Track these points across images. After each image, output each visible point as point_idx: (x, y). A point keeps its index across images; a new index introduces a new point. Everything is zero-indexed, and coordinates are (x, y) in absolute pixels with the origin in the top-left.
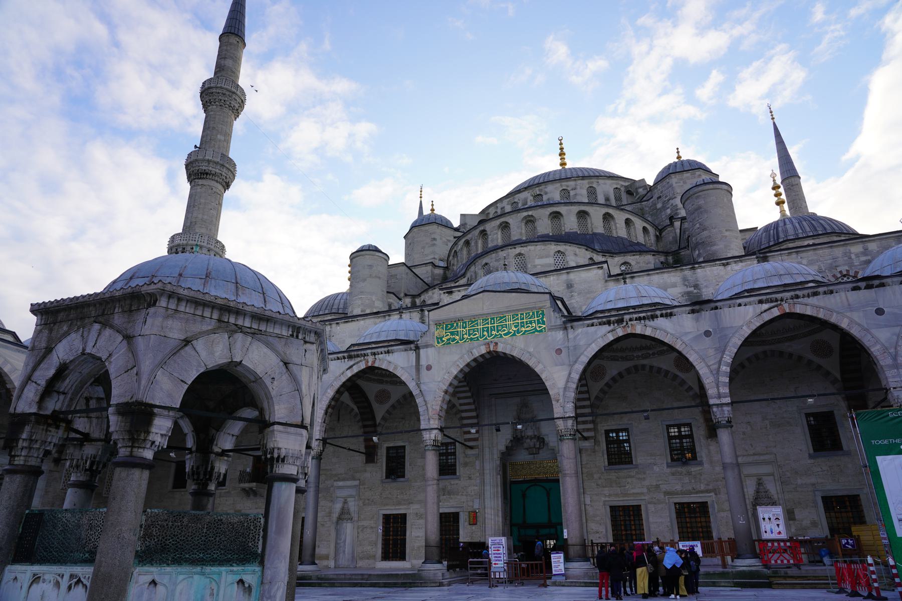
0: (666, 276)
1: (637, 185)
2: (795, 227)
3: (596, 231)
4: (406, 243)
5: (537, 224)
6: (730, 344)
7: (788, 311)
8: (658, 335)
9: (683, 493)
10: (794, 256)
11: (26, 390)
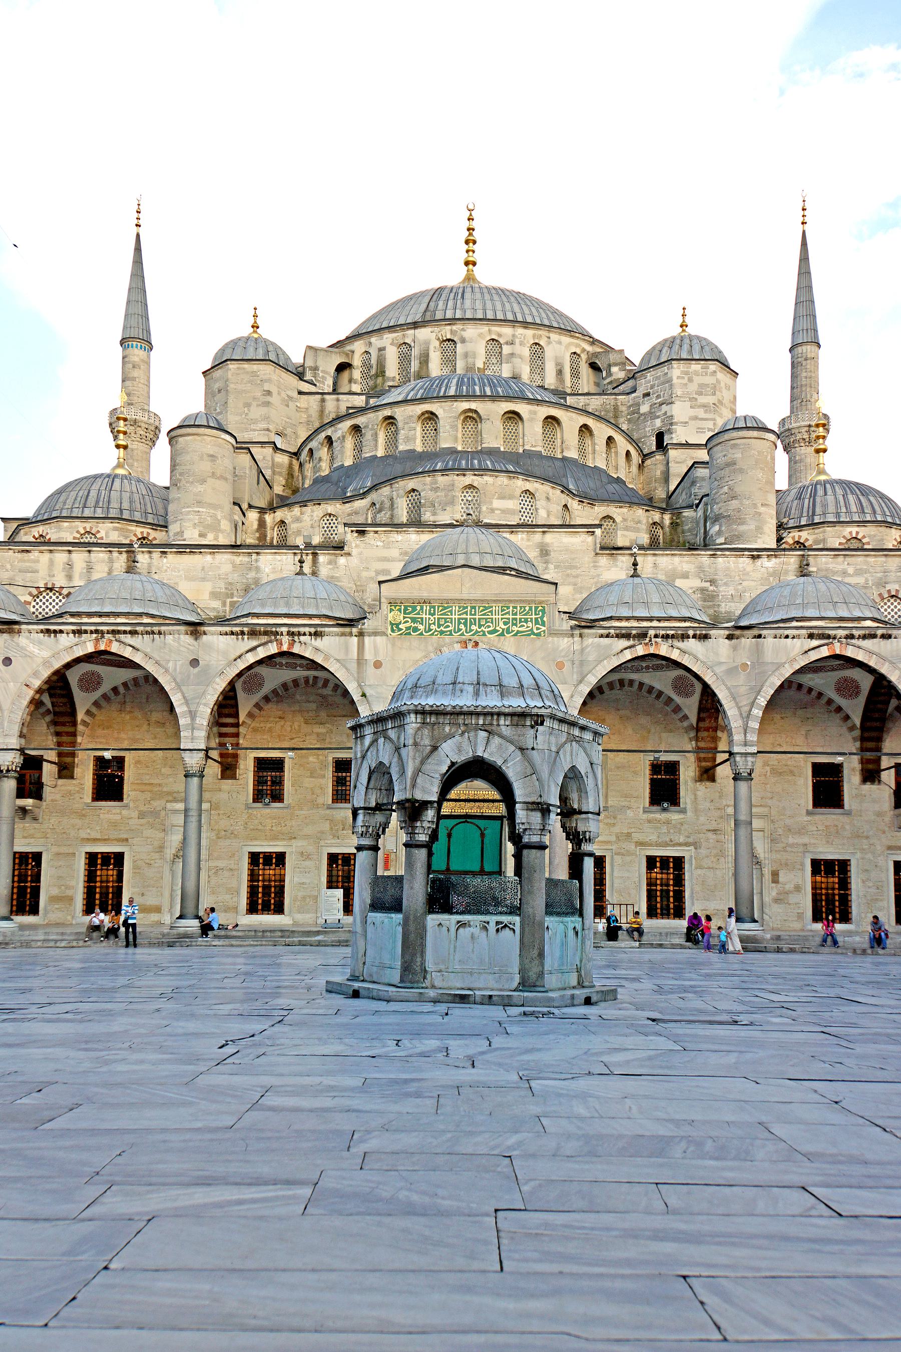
0: (677, 559)
1: (612, 357)
2: (837, 502)
3: (567, 454)
4: (207, 386)
5: (485, 426)
6: (767, 684)
7: (838, 652)
8: (686, 661)
10: (841, 559)
11: (418, 781)
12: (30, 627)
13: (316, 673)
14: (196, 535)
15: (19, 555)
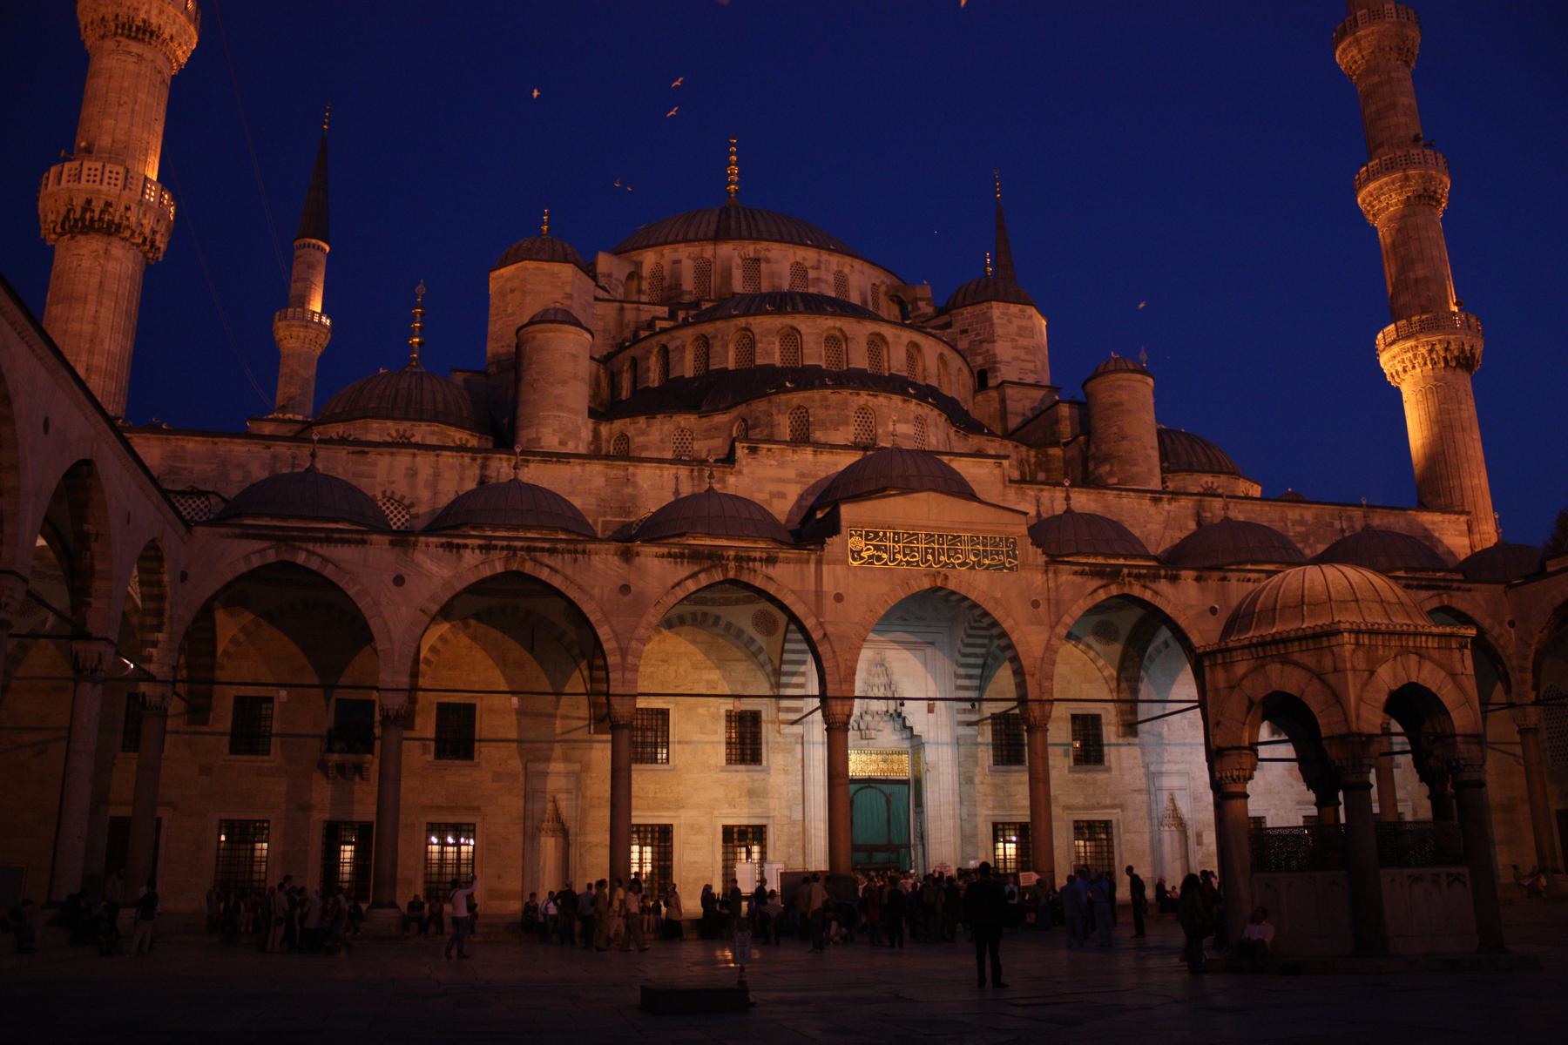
8: (1158, 602)
9: (1085, 808)
12: (431, 539)
13: (704, 609)
14: (555, 441)
15: (354, 457)
